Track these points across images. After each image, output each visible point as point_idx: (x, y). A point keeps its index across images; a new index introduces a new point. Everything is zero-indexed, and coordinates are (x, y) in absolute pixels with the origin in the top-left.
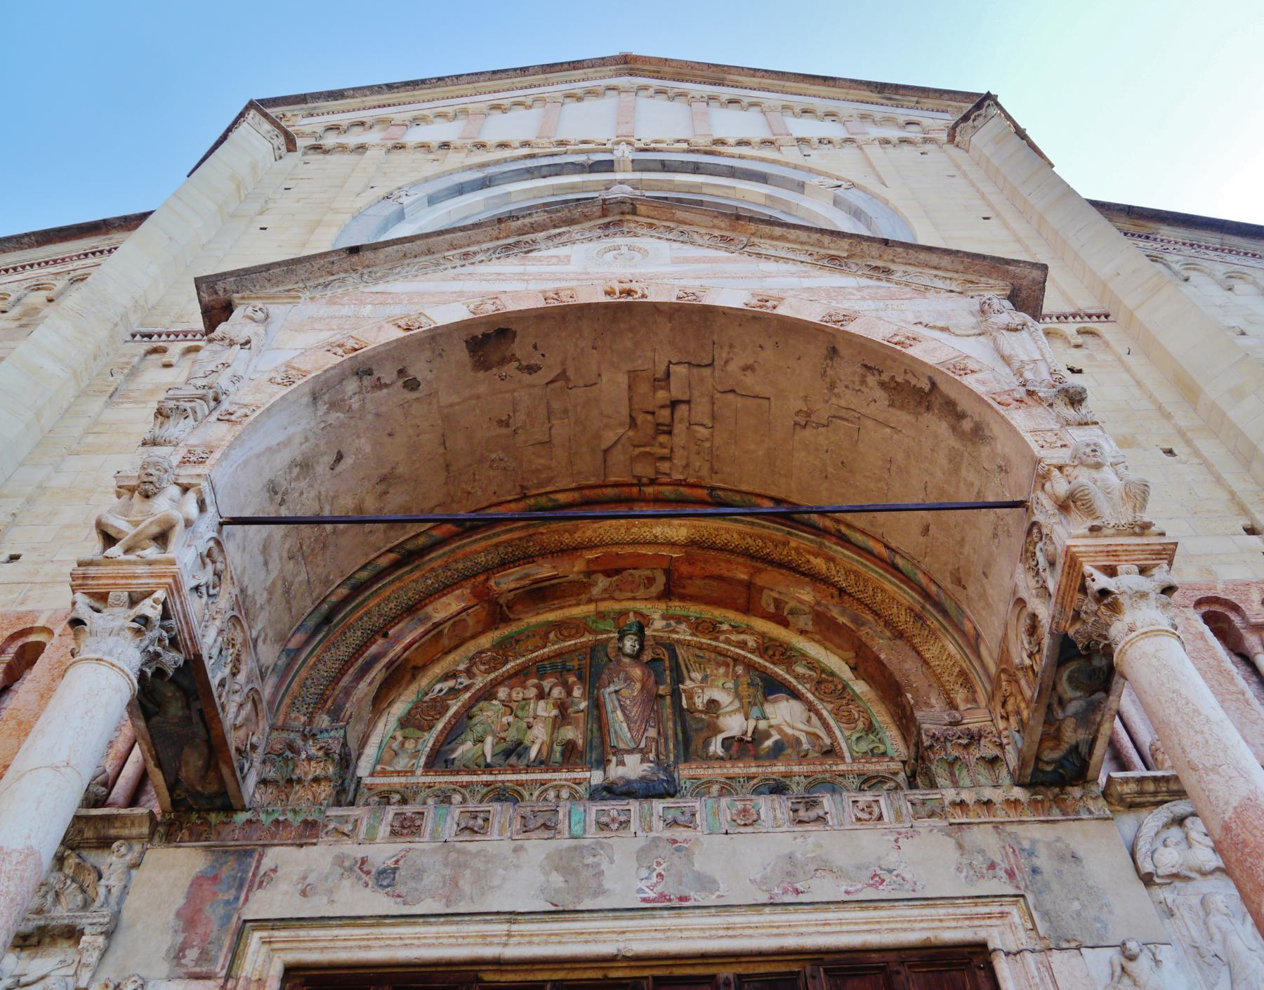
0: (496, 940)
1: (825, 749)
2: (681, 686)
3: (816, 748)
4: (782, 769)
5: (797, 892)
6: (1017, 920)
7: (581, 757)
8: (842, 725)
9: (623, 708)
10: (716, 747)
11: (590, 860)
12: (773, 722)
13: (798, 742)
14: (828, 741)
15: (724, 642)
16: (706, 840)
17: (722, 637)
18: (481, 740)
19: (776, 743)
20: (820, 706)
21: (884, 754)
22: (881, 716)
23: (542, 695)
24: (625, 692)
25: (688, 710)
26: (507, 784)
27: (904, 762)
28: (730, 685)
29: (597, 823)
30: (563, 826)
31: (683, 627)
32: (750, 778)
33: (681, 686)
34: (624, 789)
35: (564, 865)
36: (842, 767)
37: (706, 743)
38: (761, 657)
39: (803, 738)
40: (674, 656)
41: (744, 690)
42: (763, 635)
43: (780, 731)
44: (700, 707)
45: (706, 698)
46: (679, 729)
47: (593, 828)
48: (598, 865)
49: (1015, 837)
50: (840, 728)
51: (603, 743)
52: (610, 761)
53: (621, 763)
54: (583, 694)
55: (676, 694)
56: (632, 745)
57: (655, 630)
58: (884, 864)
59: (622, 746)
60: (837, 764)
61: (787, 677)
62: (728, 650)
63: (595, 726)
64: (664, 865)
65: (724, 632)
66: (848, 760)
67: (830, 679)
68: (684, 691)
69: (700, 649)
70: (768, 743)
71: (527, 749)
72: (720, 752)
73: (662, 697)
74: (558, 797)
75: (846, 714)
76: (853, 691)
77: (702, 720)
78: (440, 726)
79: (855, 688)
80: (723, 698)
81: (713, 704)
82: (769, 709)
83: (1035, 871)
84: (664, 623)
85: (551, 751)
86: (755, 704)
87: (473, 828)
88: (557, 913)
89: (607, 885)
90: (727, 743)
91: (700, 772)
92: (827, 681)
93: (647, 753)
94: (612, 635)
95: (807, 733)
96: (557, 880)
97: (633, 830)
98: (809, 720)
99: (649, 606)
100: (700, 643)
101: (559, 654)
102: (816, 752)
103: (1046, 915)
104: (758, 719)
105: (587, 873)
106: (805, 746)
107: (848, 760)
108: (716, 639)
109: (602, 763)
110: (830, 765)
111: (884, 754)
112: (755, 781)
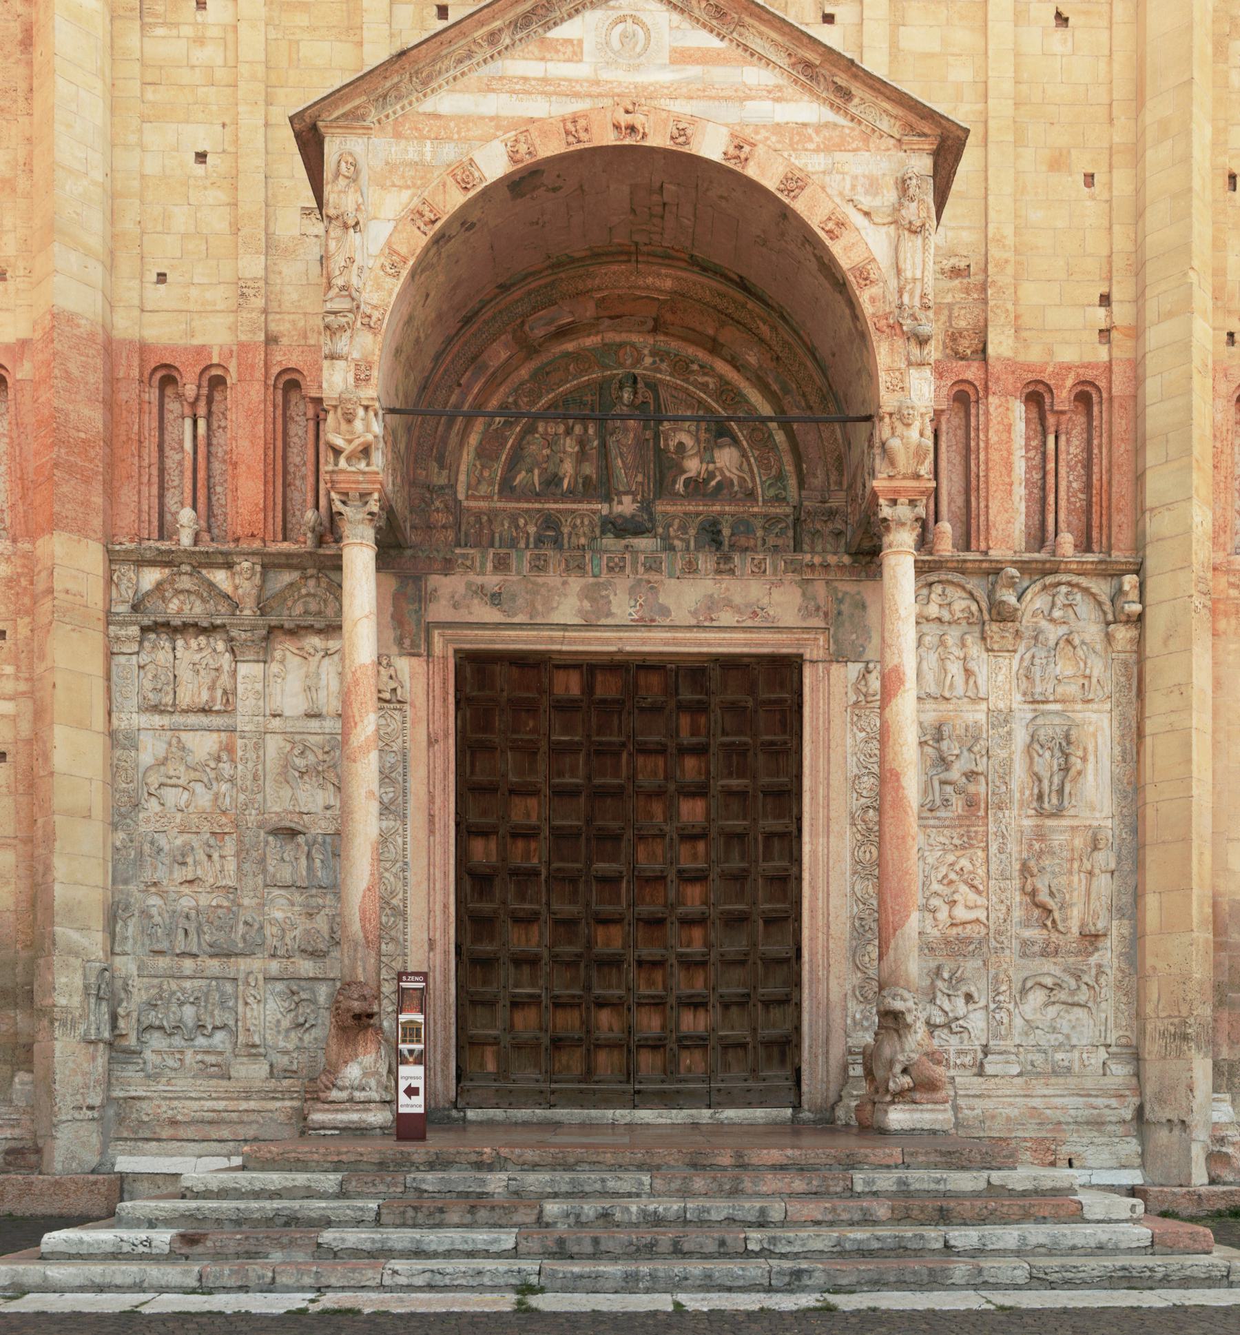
4: (719, 508)
5: (712, 620)
6: (821, 643)
10: (679, 486)
11: (604, 593)
12: (718, 465)
13: (732, 481)
14: (750, 485)
16: (667, 581)
18: (530, 471)
19: (718, 483)
21: (785, 498)
22: (789, 468)
23: (569, 432)
28: (693, 428)
30: (589, 568)
32: (698, 514)
35: (590, 594)
36: (756, 509)
37: (674, 482)
38: (717, 402)
39: (736, 482)
40: (657, 398)
41: (703, 436)
43: (722, 473)
44: (672, 449)
48: (608, 596)
49: (835, 589)
51: (609, 480)
53: (620, 502)
54: (595, 432)
55: (657, 436)
57: (645, 369)
58: (760, 604)
59: (621, 489)
70: (713, 483)
71: (561, 480)
72: (681, 490)
74: (582, 522)
78: (504, 457)
80: (688, 441)
81: (681, 446)
82: (717, 454)
83: (840, 613)
85: (576, 482)
87: (539, 566)
88: (588, 626)
89: (614, 610)
90: (687, 482)
91: (669, 508)
96: (587, 605)
98: (741, 465)
101: (578, 388)
103: (836, 642)
104: (708, 463)
105: (602, 602)
106: (736, 488)
109: (608, 499)
111: (785, 498)
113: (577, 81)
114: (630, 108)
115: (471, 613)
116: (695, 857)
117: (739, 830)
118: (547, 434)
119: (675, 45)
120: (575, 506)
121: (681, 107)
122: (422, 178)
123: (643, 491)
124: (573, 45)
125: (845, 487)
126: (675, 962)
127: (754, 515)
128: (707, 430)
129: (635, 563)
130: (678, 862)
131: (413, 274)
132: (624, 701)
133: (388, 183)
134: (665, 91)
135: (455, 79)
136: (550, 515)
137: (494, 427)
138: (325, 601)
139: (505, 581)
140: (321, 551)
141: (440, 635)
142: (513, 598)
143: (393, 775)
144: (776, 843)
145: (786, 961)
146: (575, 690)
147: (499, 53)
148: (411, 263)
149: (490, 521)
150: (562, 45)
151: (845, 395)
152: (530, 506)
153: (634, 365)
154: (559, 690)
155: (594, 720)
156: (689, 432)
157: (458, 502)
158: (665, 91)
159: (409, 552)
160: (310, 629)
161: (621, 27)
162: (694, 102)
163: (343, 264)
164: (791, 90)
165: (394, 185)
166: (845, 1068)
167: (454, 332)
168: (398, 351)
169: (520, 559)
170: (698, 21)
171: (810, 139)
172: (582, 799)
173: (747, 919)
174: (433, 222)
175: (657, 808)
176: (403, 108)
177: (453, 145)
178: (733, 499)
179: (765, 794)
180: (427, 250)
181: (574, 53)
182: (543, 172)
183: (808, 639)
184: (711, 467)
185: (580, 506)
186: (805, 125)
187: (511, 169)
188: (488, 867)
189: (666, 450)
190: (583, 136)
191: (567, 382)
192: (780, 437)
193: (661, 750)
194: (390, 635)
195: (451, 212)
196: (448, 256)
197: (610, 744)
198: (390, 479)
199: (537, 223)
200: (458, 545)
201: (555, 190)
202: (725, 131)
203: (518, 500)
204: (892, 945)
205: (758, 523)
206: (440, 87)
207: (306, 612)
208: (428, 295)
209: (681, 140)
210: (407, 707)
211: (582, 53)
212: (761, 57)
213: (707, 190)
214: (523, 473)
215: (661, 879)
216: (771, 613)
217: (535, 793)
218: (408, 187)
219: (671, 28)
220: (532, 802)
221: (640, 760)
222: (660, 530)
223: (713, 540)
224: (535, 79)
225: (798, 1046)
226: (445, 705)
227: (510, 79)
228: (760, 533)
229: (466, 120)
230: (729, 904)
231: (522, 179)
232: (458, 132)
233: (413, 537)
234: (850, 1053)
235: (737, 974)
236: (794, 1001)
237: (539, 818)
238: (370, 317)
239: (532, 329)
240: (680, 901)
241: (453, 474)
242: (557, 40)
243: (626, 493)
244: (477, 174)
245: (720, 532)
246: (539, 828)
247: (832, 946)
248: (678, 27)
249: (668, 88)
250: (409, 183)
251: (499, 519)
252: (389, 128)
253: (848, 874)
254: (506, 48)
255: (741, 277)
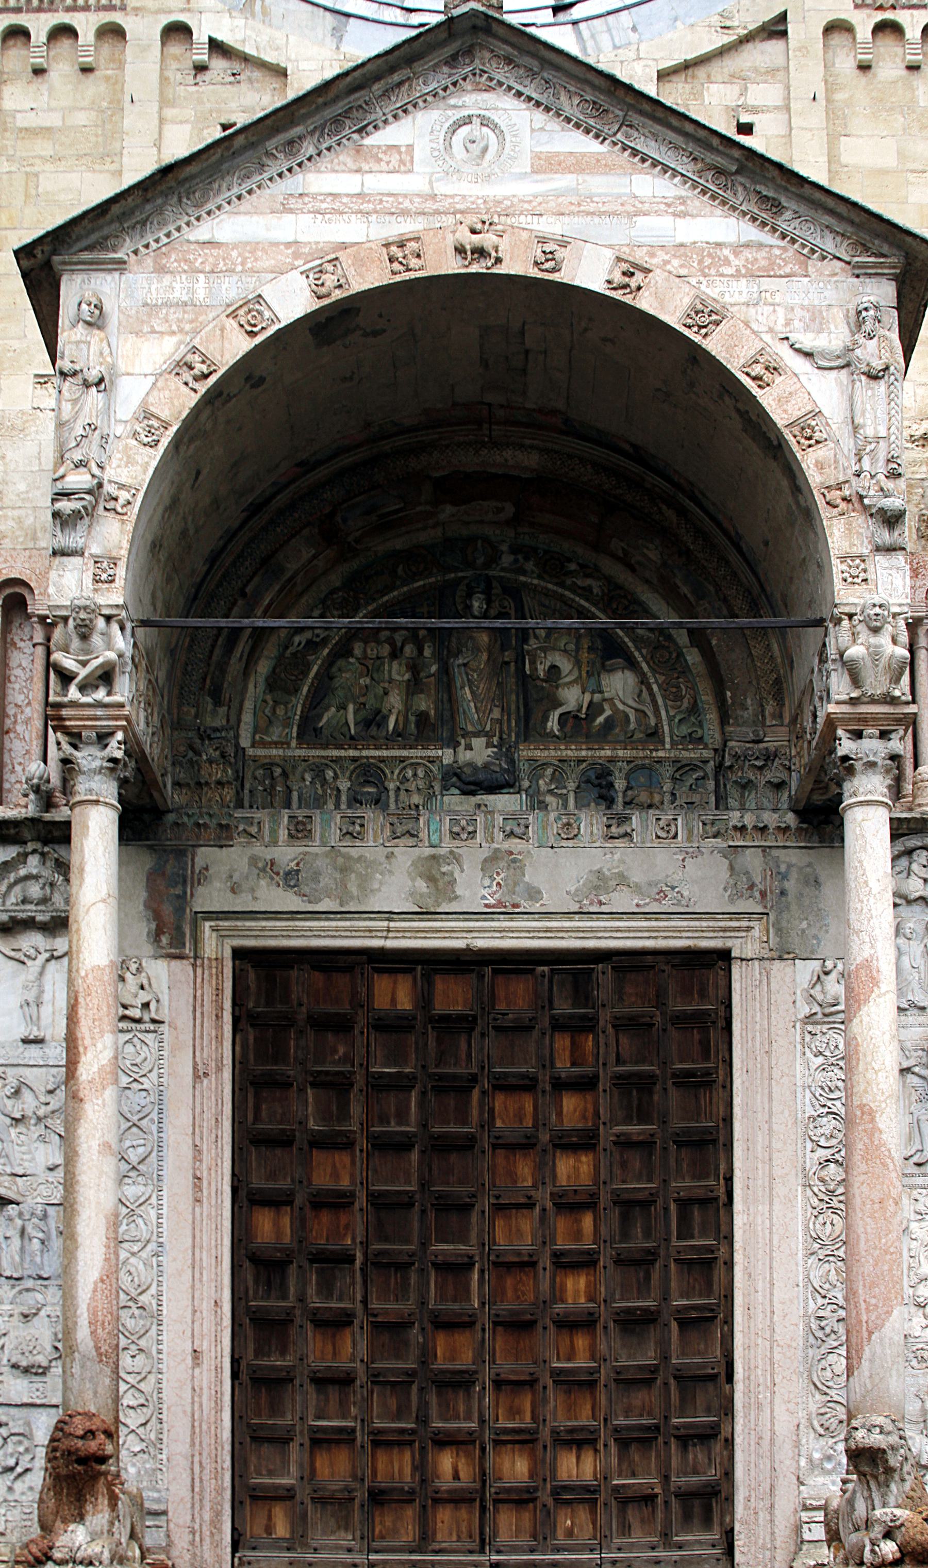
0: (379, 934)
1: (649, 731)
2: (526, 647)
3: (642, 728)
4: (609, 753)
7: (434, 731)
8: (669, 703)
9: (470, 683)
10: (553, 724)
12: (606, 695)
14: (653, 722)
15: (570, 590)
17: (569, 582)
19: (607, 720)
20: (652, 680)
21: (701, 738)
24: (473, 664)
25: (530, 676)
26: (372, 761)
27: (716, 750)
28: (572, 647)
29: (451, 832)
31: (530, 566)
32: (580, 761)
33: (526, 647)
34: (472, 779)
36: (661, 754)
37: (546, 719)
39: (632, 718)
41: (584, 655)
42: (608, 579)
44: (542, 675)
45: (548, 664)
46: (521, 701)
47: (447, 837)
50: (666, 706)
51: (453, 718)
52: (459, 744)
53: (469, 747)
56: (479, 728)
59: (470, 728)
60: (657, 750)
61: (626, 640)
62: (573, 600)
63: (445, 696)
64: (502, 875)
65: (570, 573)
66: (668, 746)
67: (667, 644)
68: (528, 652)
69: (546, 595)
70: (601, 719)
73: (507, 663)
74: (415, 775)
75: (674, 690)
76: (686, 661)
77: (543, 688)
79: (688, 658)
81: (554, 668)
84: (512, 558)
86: (593, 675)
91: (538, 753)
92: (663, 646)
93: (492, 736)
94: (460, 574)
95: (636, 710)
97: (478, 841)
99: (498, 532)
100: (546, 588)
102: (641, 732)
104: (593, 693)
106: (632, 726)
107: (668, 746)
108: (562, 585)
110: (651, 751)
112: (584, 765)
113: (405, 196)
114: (479, 226)
115: (255, 899)
116: (577, 1235)
117: (640, 1196)
118: (365, 657)
119: (538, 149)
120: (405, 753)
121: (551, 226)
122: (191, 322)
123: (501, 732)
124: (400, 153)
125: (786, 721)
126: (550, 1383)
127: (659, 761)
128: (590, 649)
129: (489, 828)
130: (553, 1242)
131: (177, 443)
132: (475, 1018)
133: (146, 329)
134: (526, 206)
135: (239, 198)
136: (369, 765)
137: (291, 650)
138: (52, 885)
139: (305, 854)
140: (48, 816)
141: (214, 929)
142: (316, 876)
143: (144, 1123)
144: (697, 1213)
145: (713, 1378)
146: (405, 1002)
147: (300, 165)
148: (174, 428)
149: (285, 774)
150: (385, 153)
151: (784, 597)
152: (342, 753)
153: (487, 565)
154: (381, 1002)
155: (432, 1043)
156: (565, 651)
157: (240, 751)
158: (526, 206)
159: (171, 817)
160: (29, 924)
161: (464, 131)
162: (566, 219)
163: (81, 432)
164: (698, 202)
165: (153, 332)
166: (798, 1529)
167: (236, 524)
168: (155, 546)
169: (326, 824)
170: (568, 120)
171: (727, 262)
172: (415, 1156)
173: (654, 1321)
174: (206, 376)
175: (525, 1171)
176: (168, 235)
177: (235, 278)
178: (629, 741)
179: (679, 1144)
180: (196, 411)
181: (402, 162)
182: (359, 310)
183: (738, 929)
184: (597, 697)
185: (412, 753)
186: (719, 245)
187: (317, 305)
188: (280, 1250)
189: (534, 677)
190: (414, 262)
191: (393, 588)
192: (693, 657)
193: (528, 1085)
194: (142, 928)
195: (231, 363)
196: (228, 422)
197: (455, 1077)
198: (142, 714)
199: (351, 379)
200: (240, 805)
201: (375, 334)
202: (609, 254)
203: (325, 747)
204: (867, 1354)
205: (667, 771)
206: (219, 208)
207: (24, 901)
208: (198, 473)
209: (548, 265)
210: (164, 1028)
211: (412, 162)
212: (655, 163)
213: (586, 330)
214: (333, 709)
215: (528, 1264)
216: (686, 893)
217: (348, 1145)
218: (173, 333)
219: (533, 130)
220: (342, 1159)
221: (499, 1101)
222: (526, 784)
223: (601, 797)
224: (348, 195)
225: (730, 1499)
226: (219, 1028)
227: (314, 197)
228: (667, 787)
229: (253, 247)
230: (628, 1300)
231: (329, 319)
232: (243, 264)
233: (173, 797)
234: (806, 1508)
235: (639, 1397)
236: (722, 1437)
237: (353, 1182)
238: (116, 499)
239: (345, 520)
240: (558, 1294)
241: (233, 713)
242: (379, 147)
243: (477, 735)
244: (267, 314)
245: (611, 785)
246: (352, 1194)
247: (777, 1357)
248: (542, 129)
249: (530, 202)
250: (174, 328)
251: (300, 769)
252: (149, 261)
253: (800, 1255)
254: (309, 159)
255: (635, 447)
